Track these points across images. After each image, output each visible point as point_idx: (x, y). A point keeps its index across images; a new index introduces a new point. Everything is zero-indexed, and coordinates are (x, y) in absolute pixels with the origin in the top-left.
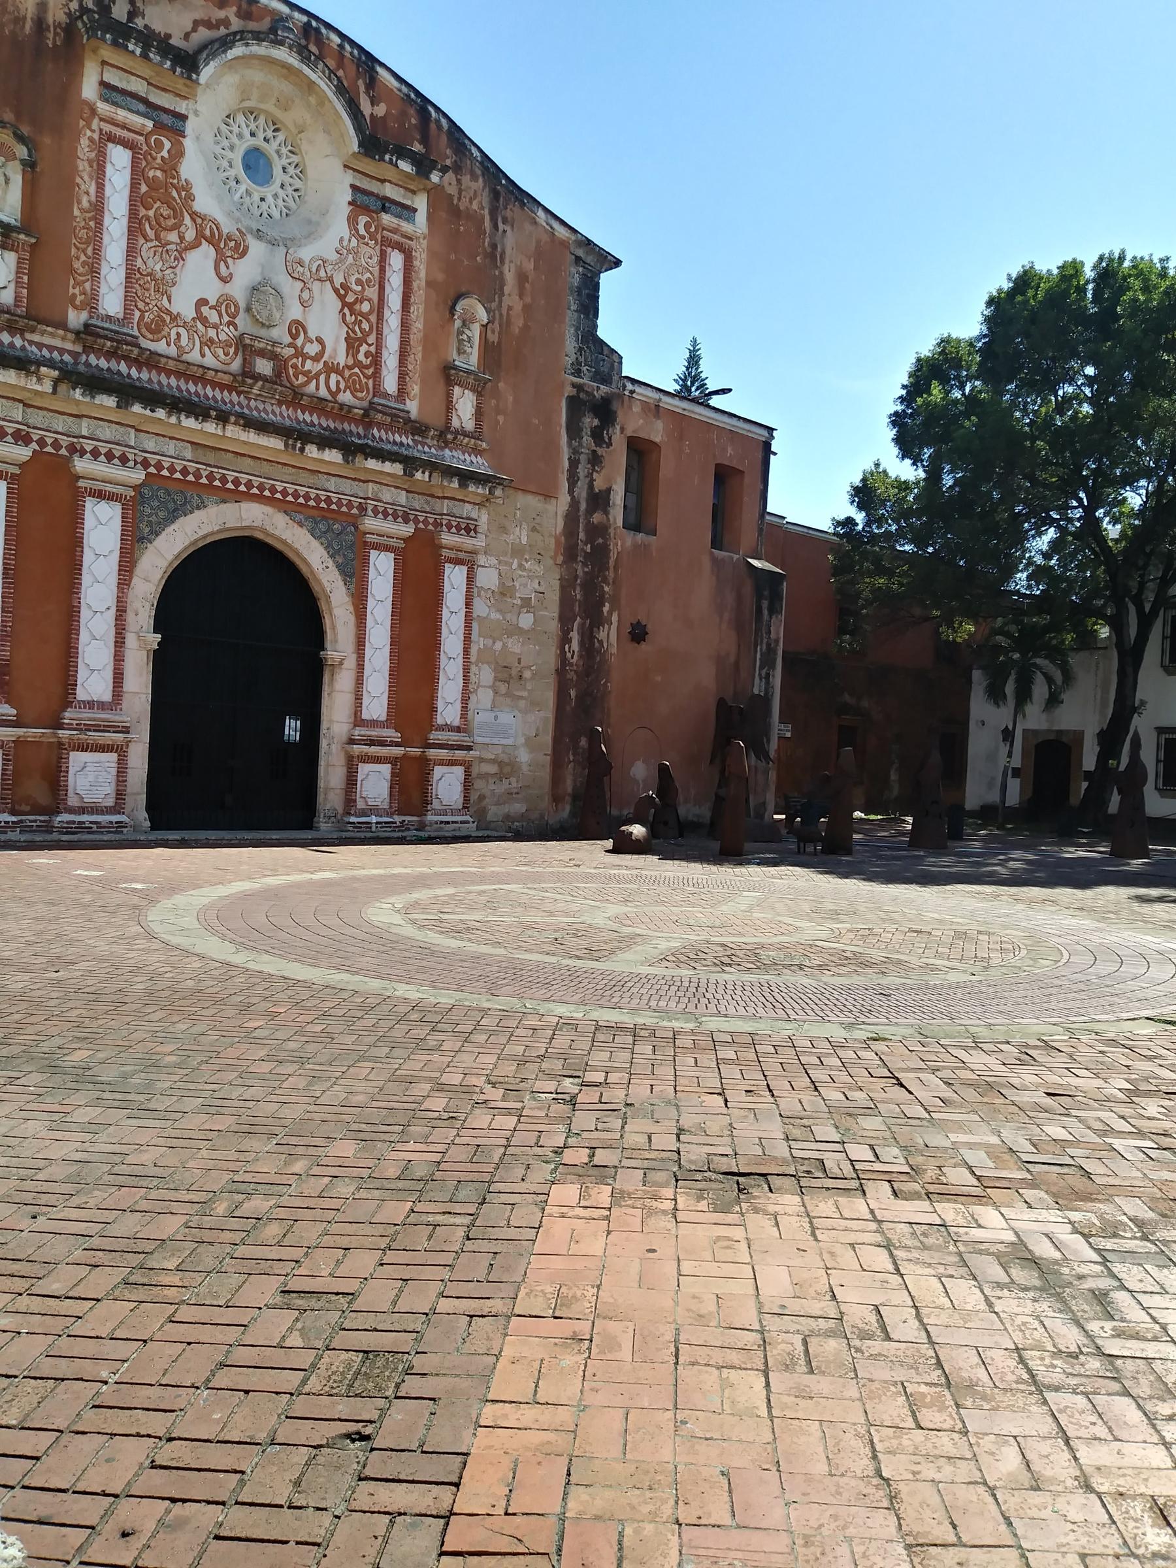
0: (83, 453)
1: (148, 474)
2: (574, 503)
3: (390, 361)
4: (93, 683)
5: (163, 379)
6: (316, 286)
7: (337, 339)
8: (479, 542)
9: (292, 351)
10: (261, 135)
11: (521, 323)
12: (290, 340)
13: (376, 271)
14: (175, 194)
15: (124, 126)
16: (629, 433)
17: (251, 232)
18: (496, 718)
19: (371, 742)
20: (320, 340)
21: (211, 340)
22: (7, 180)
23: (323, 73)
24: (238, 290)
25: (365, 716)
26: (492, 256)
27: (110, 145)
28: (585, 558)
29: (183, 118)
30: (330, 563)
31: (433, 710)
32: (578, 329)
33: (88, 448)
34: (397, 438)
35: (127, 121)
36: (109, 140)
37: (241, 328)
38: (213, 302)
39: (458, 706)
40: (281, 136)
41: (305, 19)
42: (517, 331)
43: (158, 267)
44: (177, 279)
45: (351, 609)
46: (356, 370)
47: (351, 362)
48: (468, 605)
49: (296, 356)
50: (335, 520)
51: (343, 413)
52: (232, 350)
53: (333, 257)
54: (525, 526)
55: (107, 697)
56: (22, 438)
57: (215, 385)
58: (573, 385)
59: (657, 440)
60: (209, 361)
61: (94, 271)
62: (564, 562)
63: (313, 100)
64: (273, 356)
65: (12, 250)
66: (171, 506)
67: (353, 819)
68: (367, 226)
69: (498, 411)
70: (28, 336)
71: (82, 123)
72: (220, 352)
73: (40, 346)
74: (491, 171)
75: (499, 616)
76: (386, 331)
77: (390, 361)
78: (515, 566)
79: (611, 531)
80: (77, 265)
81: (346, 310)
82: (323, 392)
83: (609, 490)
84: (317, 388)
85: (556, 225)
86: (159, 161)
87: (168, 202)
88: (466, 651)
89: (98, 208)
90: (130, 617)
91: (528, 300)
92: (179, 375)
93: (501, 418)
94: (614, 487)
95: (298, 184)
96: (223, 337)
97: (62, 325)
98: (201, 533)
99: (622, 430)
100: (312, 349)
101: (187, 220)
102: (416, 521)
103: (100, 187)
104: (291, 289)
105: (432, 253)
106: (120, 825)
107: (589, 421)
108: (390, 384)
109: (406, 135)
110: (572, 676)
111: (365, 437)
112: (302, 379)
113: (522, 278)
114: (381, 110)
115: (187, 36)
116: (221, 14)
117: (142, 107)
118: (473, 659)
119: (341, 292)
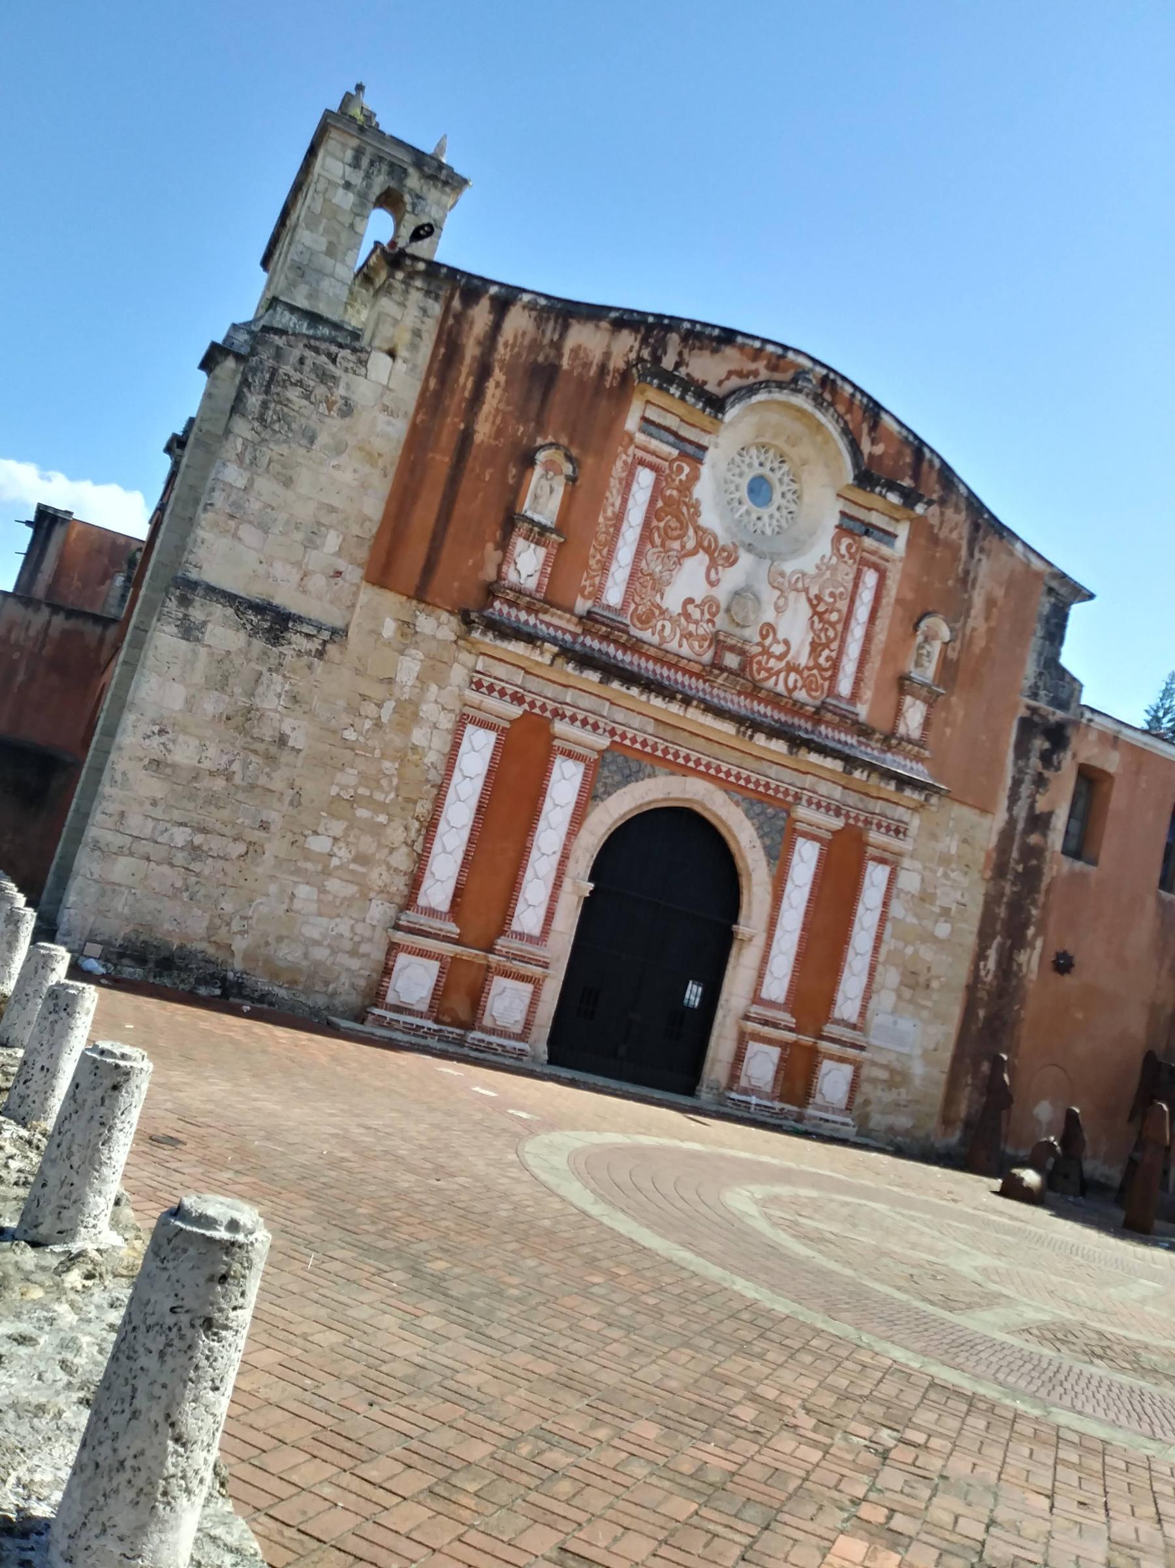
0: (563, 717)
1: (613, 742)
2: (1012, 821)
3: (849, 667)
4: (528, 916)
5: (643, 662)
6: (792, 596)
7: (803, 642)
8: (906, 845)
9: (759, 649)
10: (768, 465)
13: (850, 586)
14: (684, 510)
15: (654, 453)
16: (1081, 759)
18: (895, 1023)
19: (766, 1023)
20: (786, 642)
21: (690, 634)
22: (552, 490)
24: (722, 594)
25: (764, 994)
27: (640, 468)
29: (704, 449)
30: (758, 843)
31: (831, 1002)
32: (1040, 654)
33: (568, 714)
34: (843, 737)
37: (718, 625)
38: (698, 602)
39: (858, 1003)
40: (785, 467)
41: (824, 372)
45: (770, 888)
47: (811, 664)
48: (885, 904)
49: (762, 654)
50: (770, 805)
51: (796, 708)
52: (706, 644)
53: (812, 571)
54: (956, 836)
55: (536, 931)
56: (517, 699)
57: (685, 671)
58: (1028, 707)
60: (685, 651)
61: (605, 568)
62: (992, 878)
63: (819, 438)
66: (627, 772)
67: (734, 1095)
68: (849, 547)
69: (946, 723)
70: (541, 616)
71: (620, 449)
72: (696, 644)
73: (549, 625)
74: (975, 506)
75: (915, 921)
76: (849, 639)
77: (849, 667)
79: (1048, 855)
80: (592, 562)
81: (816, 619)
82: (780, 688)
83: (1050, 814)
85: (1033, 558)
87: (678, 517)
88: (876, 949)
89: (619, 518)
90: (571, 864)
91: (993, 623)
92: (657, 660)
93: (948, 731)
95: (793, 507)
96: (701, 632)
97: (570, 610)
98: (647, 799)
99: (1074, 756)
100: (778, 649)
101: (691, 532)
102: (847, 816)
103: (625, 501)
104: (769, 595)
105: (906, 575)
106: (522, 1053)
107: (1040, 744)
108: (845, 687)
109: (898, 470)
110: (983, 995)
111: (813, 732)
112: (763, 674)
113: (991, 603)
114: (879, 449)
115: (720, 383)
116: (752, 366)
117: (671, 439)
118: (882, 957)
119: (814, 602)
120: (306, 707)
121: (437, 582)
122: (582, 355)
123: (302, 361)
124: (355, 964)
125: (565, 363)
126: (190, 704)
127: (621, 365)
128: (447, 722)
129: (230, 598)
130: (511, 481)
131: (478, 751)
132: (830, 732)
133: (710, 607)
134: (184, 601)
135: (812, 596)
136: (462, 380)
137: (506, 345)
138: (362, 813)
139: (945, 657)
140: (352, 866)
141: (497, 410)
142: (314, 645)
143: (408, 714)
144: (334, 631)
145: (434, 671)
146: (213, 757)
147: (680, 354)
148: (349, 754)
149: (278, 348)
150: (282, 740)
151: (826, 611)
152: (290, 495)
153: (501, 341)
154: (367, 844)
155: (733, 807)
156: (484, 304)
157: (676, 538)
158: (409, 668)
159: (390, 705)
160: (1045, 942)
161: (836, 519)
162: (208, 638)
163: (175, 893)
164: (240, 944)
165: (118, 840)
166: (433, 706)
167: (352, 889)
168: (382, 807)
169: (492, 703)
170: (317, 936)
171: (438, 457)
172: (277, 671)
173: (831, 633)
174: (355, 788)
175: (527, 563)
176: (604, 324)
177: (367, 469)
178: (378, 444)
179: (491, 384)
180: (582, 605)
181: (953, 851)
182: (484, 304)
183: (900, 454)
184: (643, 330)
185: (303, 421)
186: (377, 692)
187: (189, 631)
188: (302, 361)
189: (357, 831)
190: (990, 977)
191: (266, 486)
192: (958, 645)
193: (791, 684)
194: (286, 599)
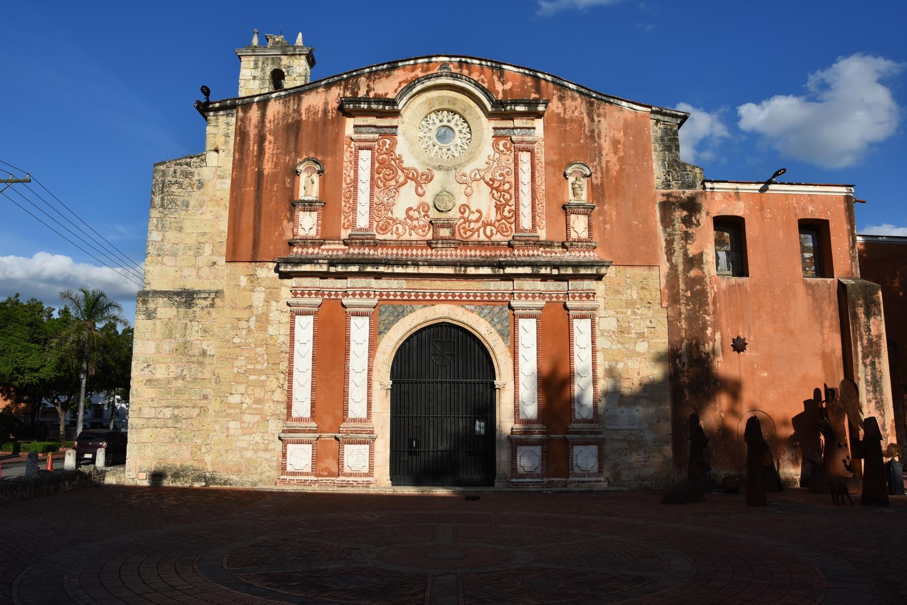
2: (673, 267)
4: (356, 408)
5: (390, 251)
7: (489, 208)
10: (445, 120)
11: (617, 168)
14: (393, 163)
15: (365, 141)
16: (715, 213)
17: (435, 168)
20: (478, 211)
21: (415, 227)
24: (429, 199)
26: (592, 137)
28: (687, 300)
30: (493, 330)
34: (531, 252)
41: (458, 59)
43: (385, 199)
46: (503, 221)
47: (499, 217)
48: (593, 342)
49: (465, 223)
51: (496, 245)
52: (427, 229)
54: (634, 287)
55: (364, 415)
58: (663, 195)
59: (740, 214)
60: (414, 237)
61: (354, 210)
62: (669, 306)
64: (450, 226)
66: (396, 314)
68: (505, 145)
69: (605, 222)
70: (323, 247)
71: (346, 146)
72: (420, 231)
73: (328, 250)
75: (620, 346)
76: (521, 195)
78: (629, 312)
79: (707, 280)
81: (494, 191)
82: (482, 238)
83: (701, 254)
89: (355, 181)
90: (375, 374)
91: (621, 154)
92: (398, 247)
93: (608, 227)
94: (705, 251)
96: (421, 223)
99: (708, 214)
103: (356, 171)
104: (459, 191)
107: (679, 214)
112: (469, 233)
113: (615, 143)
114: (508, 86)
115: (396, 91)
117: (373, 129)
120: (212, 333)
121: (262, 250)
122: (312, 109)
123: (175, 172)
124: (268, 455)
125: (304, 117)
126: (157, 348)
127: (336, 105)
128: (286, 318)
129: (164, 294)
131: (305, 327)
132: (521, 252)
133: (424, 208)
134: (145, 302)
136: (251, 148)
137: (270, 122)
138: (252, 378)
140: (254, 406)
141: (273, 154)
142: (209, 302)
143: (264, 321)
144: (217, 292)
145: (272, 295)
146: (174, 370)
147: (368, 86)
148: (238, 350)
149: (163, 171)
150: (204, 353)
152: (183, 235)
153: (267, 121)
154: (259, 393)
155: (470, 314)
156: (255, 107)
158: (258, 298)
159: (253, 319)
160: (722, 335)
161: (492, 133)
162: (159, 315)
163: (172, 440)
164: (208, 458)
165: (140, 422)
166: (277, 312)
167: (258, 418)
168: (262, 372)
169: (306, 300)
170: (245, 446)
172: (193, 320)
173: (507, 196)
174: (245, 366)
176: (320, 90)
177: (217, 208)
178: (219, 194)
179: (267, 143)
180: (344, 234)
181: (635, 296)
182: (255, 107)
184: (343, 83)
185: (182, 199)
186: (245, 314)
187: (150, 315)
188: (175, 172)
189: (252, 388)
190: (686, 367)
191: (171, 235)
192: (599, 174)
193: (488, 233)
194: (192, 284)
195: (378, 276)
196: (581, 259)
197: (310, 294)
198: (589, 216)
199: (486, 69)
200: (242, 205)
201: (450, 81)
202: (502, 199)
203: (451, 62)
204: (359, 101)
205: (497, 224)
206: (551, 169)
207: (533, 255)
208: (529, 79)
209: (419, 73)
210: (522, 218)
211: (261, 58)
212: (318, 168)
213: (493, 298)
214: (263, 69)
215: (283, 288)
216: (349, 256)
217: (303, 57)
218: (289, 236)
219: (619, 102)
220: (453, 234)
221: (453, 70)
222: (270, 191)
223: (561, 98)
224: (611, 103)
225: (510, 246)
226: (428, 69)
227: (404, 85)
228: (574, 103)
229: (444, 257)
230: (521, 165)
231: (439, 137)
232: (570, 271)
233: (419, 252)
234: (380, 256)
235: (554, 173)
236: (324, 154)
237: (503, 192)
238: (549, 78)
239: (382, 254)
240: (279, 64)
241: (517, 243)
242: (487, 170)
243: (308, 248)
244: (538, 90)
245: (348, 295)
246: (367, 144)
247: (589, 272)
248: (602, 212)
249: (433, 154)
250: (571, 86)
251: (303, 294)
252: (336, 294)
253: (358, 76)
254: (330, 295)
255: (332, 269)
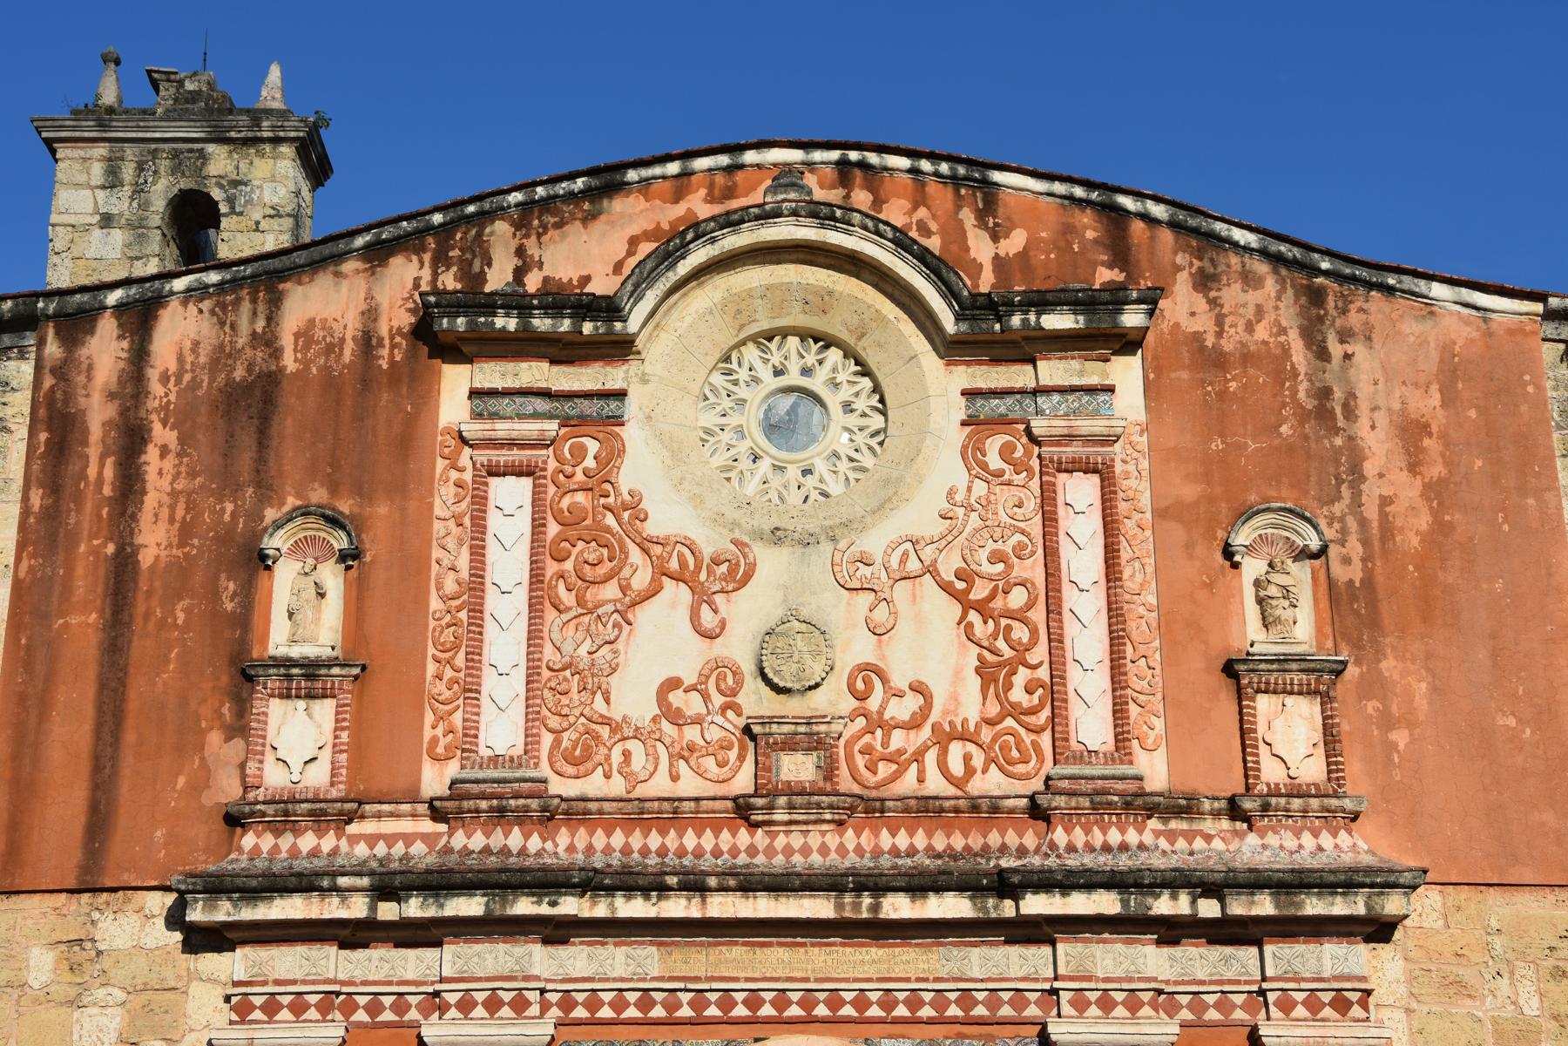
3: (1089, 685)
5: (599, 839)
6: (901, 591)
7: (958, 674)
10: (794, 367)
11: (1424, 521)
12: (854, 703)
13: (1035, 527)
14: (610, 520)
15: (511, 444)
17: (759, 536)
20: (918, 688)
21: (691, 748)
23: (865, 228)
24: (739, 648)
26: (1323, 414)
27: (494, 482)
34: (1114, 837)
35: (514, 434)
36: (491, 474)
41: (835, 155)
42: (1415, 541)
44: (621, 659)
46: (1009, 722)
47: (993, 709)
51: (987, 810)
52: (733, 755)
60: (689, 785)
61: (470, 690)
65: (325, 696)
68: (1006, 452)
69: (1387, 722)
70: (353, 828)
71: (440, 464)
72: (710, 763)
73: (372, 840)
76: (1071, 628)
77: (1089, 685)
81: (973, 616)
82: (936, 784)
84: (921, 780)
86: (580, 476)
89: (476, 585)
91: (1436, 470)
93: (1400, 737)
96: (714, 734)
97: (412, 796)
104: (845, 616)
108: (1092, 726)
112: (884, 770)
113: (1411, 432)
114: (1014, 243)
115: (618, 267)
117: (541, 405)
119: (959, 591)
121: (120, 845)
122: (319, 334)
125: (289, 362)
127: (406, 320)
130: (229, 606)
132: (1079, 836)
135: (948, 576)
136: (92, 472)
137: (165, 379)
139: (1331, 583)
141: (174, 494)
147: (520, 252)
151: (992, 596)
153: (153, 375)
156: (107, 326)
157: (606, 579)
161: (959, 409)
171: (74, 620)
173: (1021, 633)
175: (299, 742)
176: (350, 266)
179: (151, 454)
180: (434, 780)
182: (107, 326)
183: (1068, 230)
184: (431, 242)
192: (1355, 548)
193: (957, 768)
195: (557, 932)
196: (1306, 860)
197: (298, 1008)
198: (1326, 698)
199: (933, 188)
200: (50, 679)
201: (807, 232)
202: (1001, 644)
203: (810, 165)
204: (490, 305)
205: (986, 734)
206: (1177, 532)
207: (1124, 847)
208: (1086, 218)
209: (699, 206)
210: (1076, 710)
211: (130, 151)
212: (340, 541)
213: (980, 1011)
214: (138, 190)
215: (196, 988)
216: (452, 861)
217: (287, 150)
218: (228, 790)
219: (1421, 286)
220: (829, 771)
221: (819, 194)
222: (162, 624)
223: (1205, 282)
224: (1390, 290)
225: (1037, 812)
226: (729, 193)
227: (646, 248)
228: (1253, 297)
229: (797, 859)
230: (1067, 522)
231: (774, 428)
232: (1264, 905)
233: (708, 841)
234: (565, 858)
235: (1189, 546)
236: (362, 491)
237: (1006, 619)
238: (1158, 211)
239: (571, 848)
240: (199, 173)
241: (1061, 801)
242: (944, 541)
243: (298, 833)
244: (1121, 254)
245: (443, 1008)
246: (516, 456)
247: (1339, 907)
248: (1374, 686)
249: (751, 488)
250: (1239, 235)
251: (271, 1008)
252: (400, 1007)
253: (485, 217)
254: (374, 1008)
255: (388, 911)
